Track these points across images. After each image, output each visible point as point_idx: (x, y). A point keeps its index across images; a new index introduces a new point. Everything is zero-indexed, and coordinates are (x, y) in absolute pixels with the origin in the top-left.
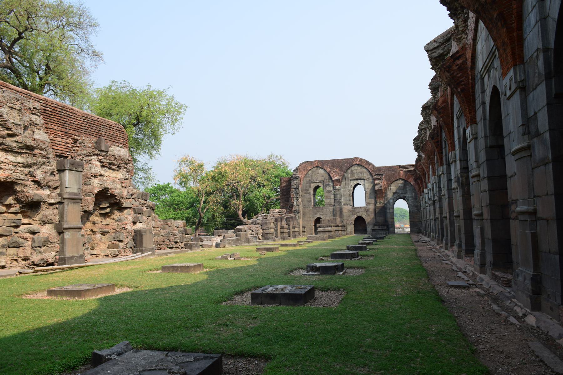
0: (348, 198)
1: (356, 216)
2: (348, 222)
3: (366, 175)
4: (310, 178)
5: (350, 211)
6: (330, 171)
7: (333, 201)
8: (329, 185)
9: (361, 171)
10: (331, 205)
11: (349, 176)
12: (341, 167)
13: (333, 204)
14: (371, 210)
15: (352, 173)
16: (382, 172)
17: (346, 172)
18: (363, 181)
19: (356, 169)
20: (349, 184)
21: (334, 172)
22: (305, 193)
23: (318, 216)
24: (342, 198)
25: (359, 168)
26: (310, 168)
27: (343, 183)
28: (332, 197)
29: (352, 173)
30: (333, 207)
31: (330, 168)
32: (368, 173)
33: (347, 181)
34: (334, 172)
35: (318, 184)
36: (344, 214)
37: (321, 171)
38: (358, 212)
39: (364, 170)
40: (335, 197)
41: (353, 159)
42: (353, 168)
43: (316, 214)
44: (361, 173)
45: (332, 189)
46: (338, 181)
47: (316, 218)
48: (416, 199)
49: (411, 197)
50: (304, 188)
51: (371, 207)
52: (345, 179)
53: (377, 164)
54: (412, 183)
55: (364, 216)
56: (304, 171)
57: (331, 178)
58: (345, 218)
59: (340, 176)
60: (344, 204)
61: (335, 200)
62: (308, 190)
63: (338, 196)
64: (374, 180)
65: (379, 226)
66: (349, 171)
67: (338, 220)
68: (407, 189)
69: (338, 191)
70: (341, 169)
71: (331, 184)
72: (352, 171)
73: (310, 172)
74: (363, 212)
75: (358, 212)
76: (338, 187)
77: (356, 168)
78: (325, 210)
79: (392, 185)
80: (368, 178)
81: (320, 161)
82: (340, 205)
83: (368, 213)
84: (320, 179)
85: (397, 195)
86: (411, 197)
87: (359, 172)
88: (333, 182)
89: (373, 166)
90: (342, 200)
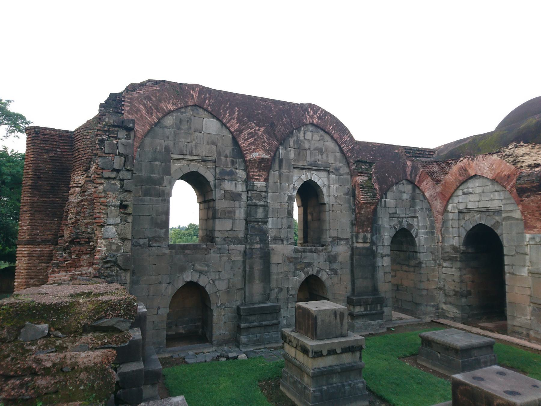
0: (285, 221)
1: (303, 277)
2: (282, 295)
3: (333, 159)
4: (170, 143)
5: (290, 260)
6: (240, 131)
7: (240, 226)
8: (231, 173)
9: (320, 145)
10: (237, 241)
11: (292, 155)
12: (273, 125)
13: (241, 235)
14: (340, 259)
15: (300, 149)
16: (368, 158)
17: (283, 142)
18: (324, 174)
19: (309, 137)
20: (289, 179)
21: (251, 135)
22: (147, 193)
23: (189, 276)
24: (270, 220)
25: (316, 137)
26: (171, 107)
27: (274, 175)
28: (240, 214)
29: (300, 149)
30: (241, 247)
31: (239, 121)
32: (339, 155)
33: (284, 171)
34: (251, 135)
35: (194, 167)
36: (274, 269)
37: (211, 125)
38: (309, 265)
39: (330, 144)
40: (248, 214)
41: (305, 108)
42: (301, 135)
43: (182, 270)
44: (321, 151)
45: (241, 188)
46: (265, 166)
47: (181, 284)
48: (433, 233)
49: (425, 227)
50: (145, 174)
51: (342, 251)
52: (281, 161)
53: (360, 134)
54: (427, 194)
55: (324, 276)
56: (150, 112)
57: (239, 153)
58: (273, 284)
59: (267, 151)
60: (276, 239)
61: (247, 222)
62: (160, 182)
63: (260, 213)
64: (353, 174)
65: (365, 304)
66: (291, 142)
67: (257, 287)
68: (418, 207)
69: (260, 198)
70: (271, 132)
71: (241, 174)
72: (298, 141)
73: (169, 121)
74: (321, 266)
75: (309, 265)
76: (259, 184)
77: (309, 135)
78: (214, 256)
79: (390, 195)
80: (337, 170)
81: (209, 90)
82: (264, 241)
83: (335, 266)
84: (204, 150)
85: (395, 221)
86: (425, 227)
87: (316, 149)
88: (248, 166)
89: (351, 138)
90: (270, 226)
